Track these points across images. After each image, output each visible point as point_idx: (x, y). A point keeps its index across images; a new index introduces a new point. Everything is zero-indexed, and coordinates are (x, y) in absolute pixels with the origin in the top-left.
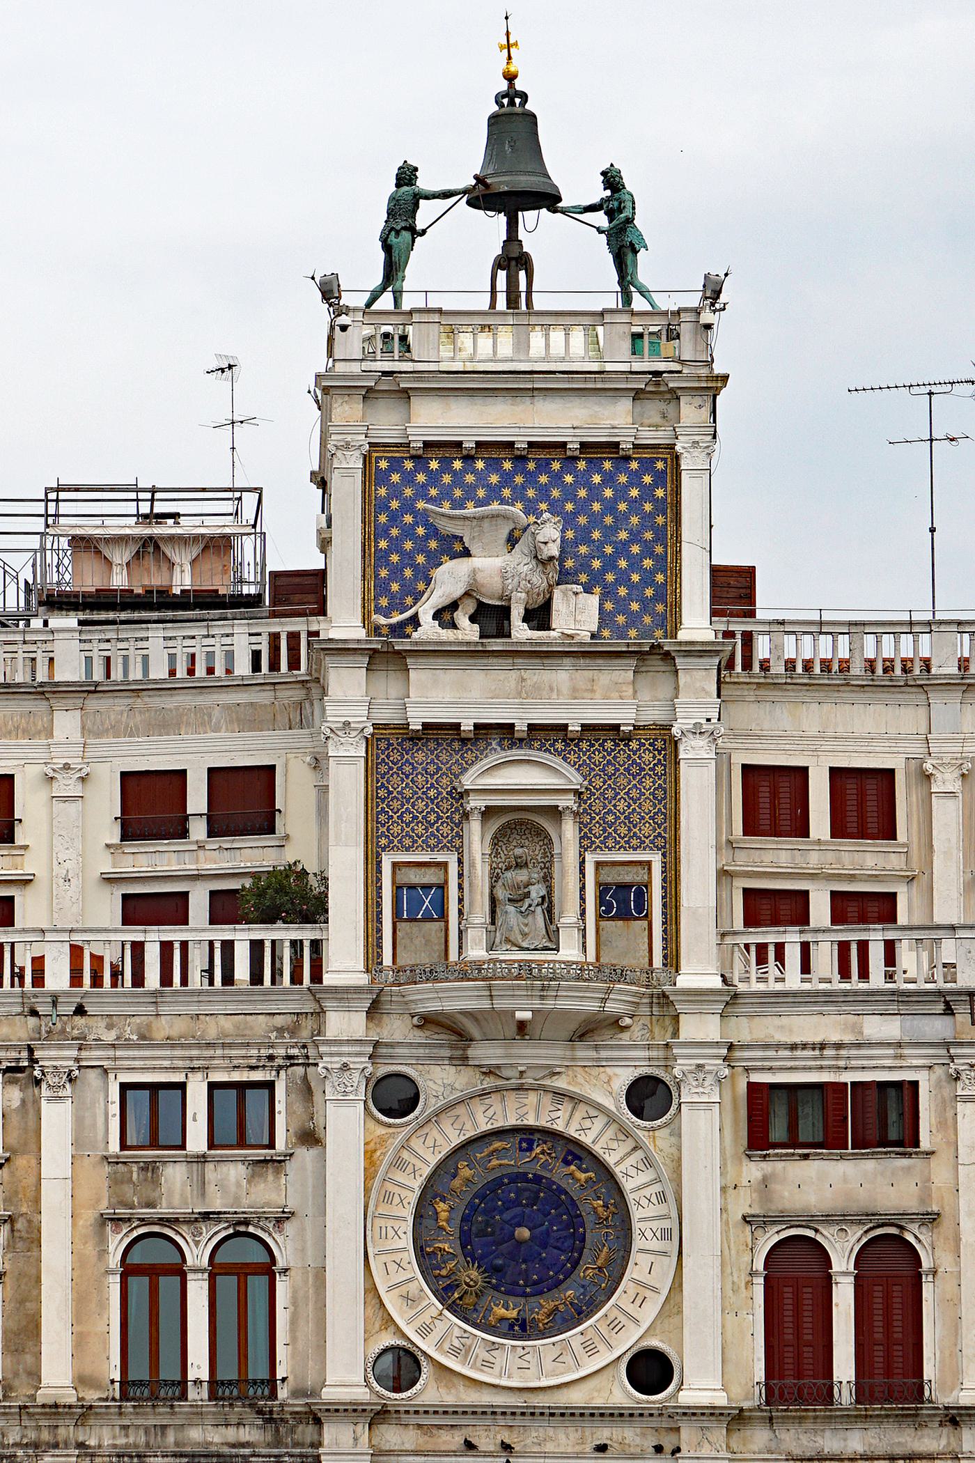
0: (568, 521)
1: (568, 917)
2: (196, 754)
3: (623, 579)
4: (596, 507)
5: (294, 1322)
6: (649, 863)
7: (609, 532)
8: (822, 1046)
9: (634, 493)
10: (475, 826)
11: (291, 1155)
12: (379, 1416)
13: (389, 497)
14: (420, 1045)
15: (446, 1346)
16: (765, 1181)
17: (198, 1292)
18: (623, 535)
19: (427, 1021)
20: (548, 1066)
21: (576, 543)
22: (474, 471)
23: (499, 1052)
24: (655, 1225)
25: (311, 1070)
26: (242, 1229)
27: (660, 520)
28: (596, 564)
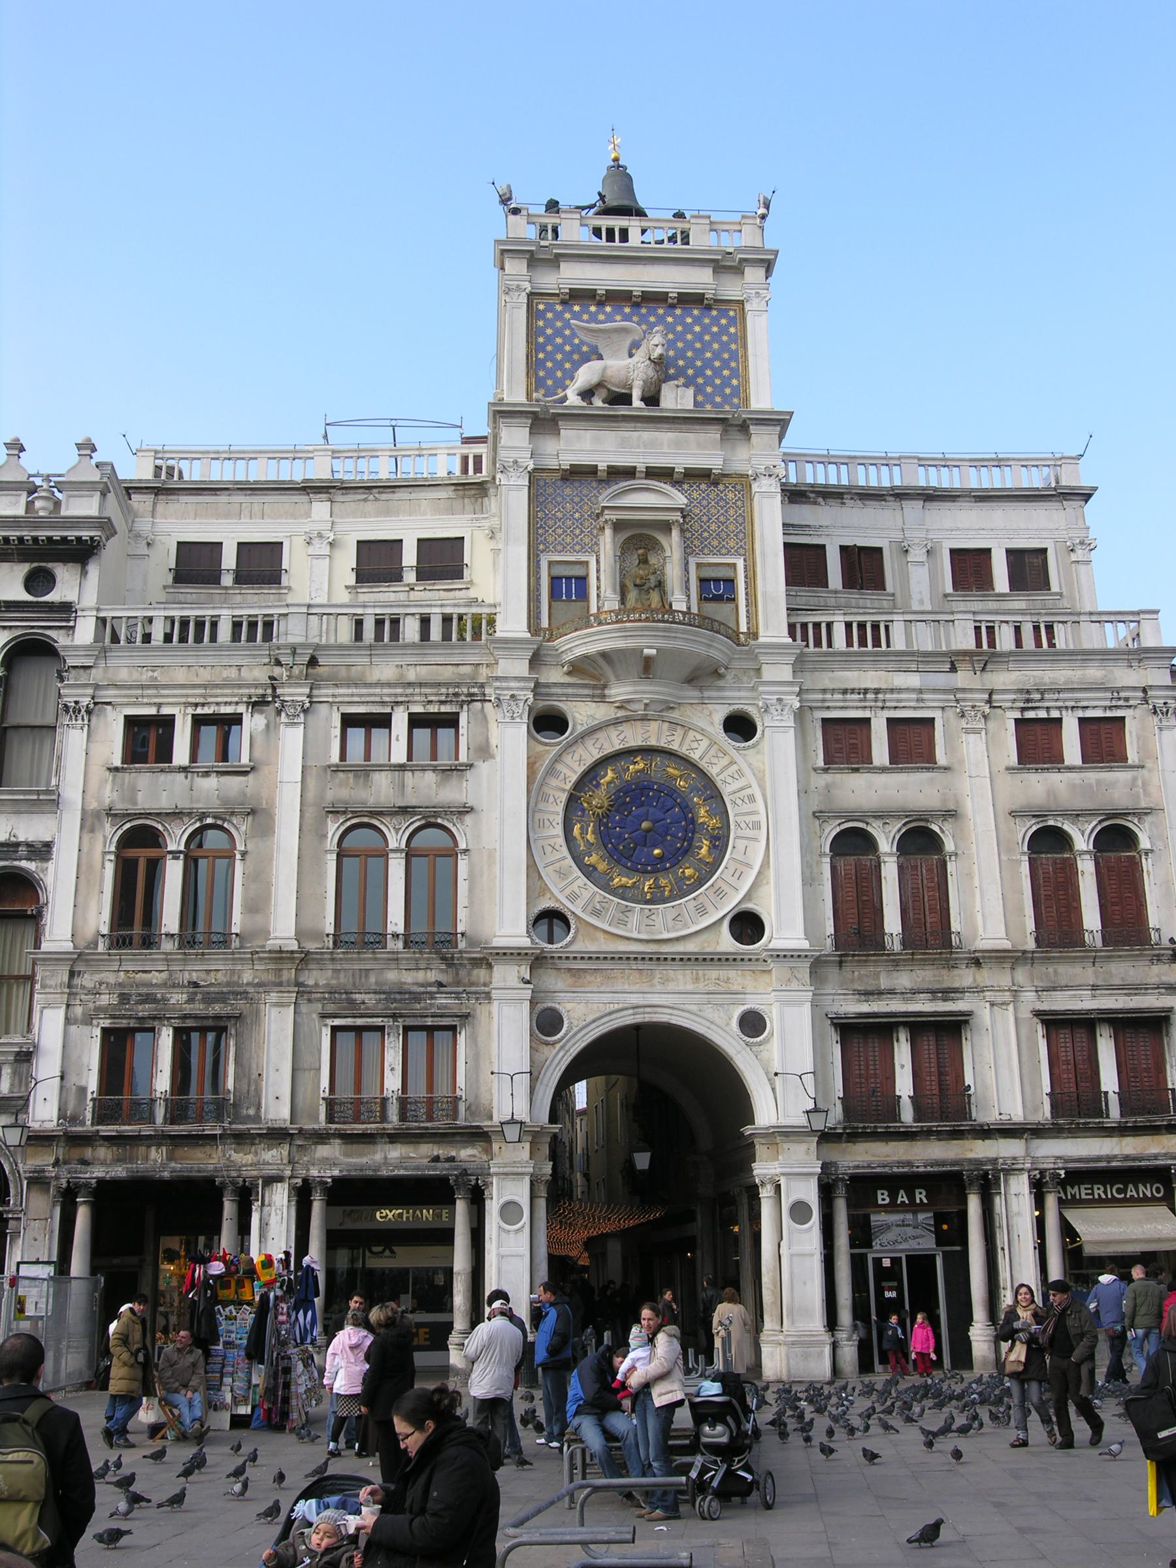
0: (670, 344)
2: (409, 527)
3: (709, 381)
4: (689, 337)
5: (471, 890)
6: (735, 564)
7: (699, 353)
8: (866, 691)
9: (715, 329)
10: (608, 532)
11: (471, 766)
12: (538, 961)
13: (546, 327)
14: (569, 685)
15: (590, 908)
16: (828, 788)
17: (396, 868)
18: (708, 355)
19: (578, 667)
20: (665, 701)
21: (676, 358)
22: (604, 313)
23: (629, 689)
24: (748, 818)
25: (488, 705)
26: (432, 820)
27: (733, 347)
28: (690, 372)
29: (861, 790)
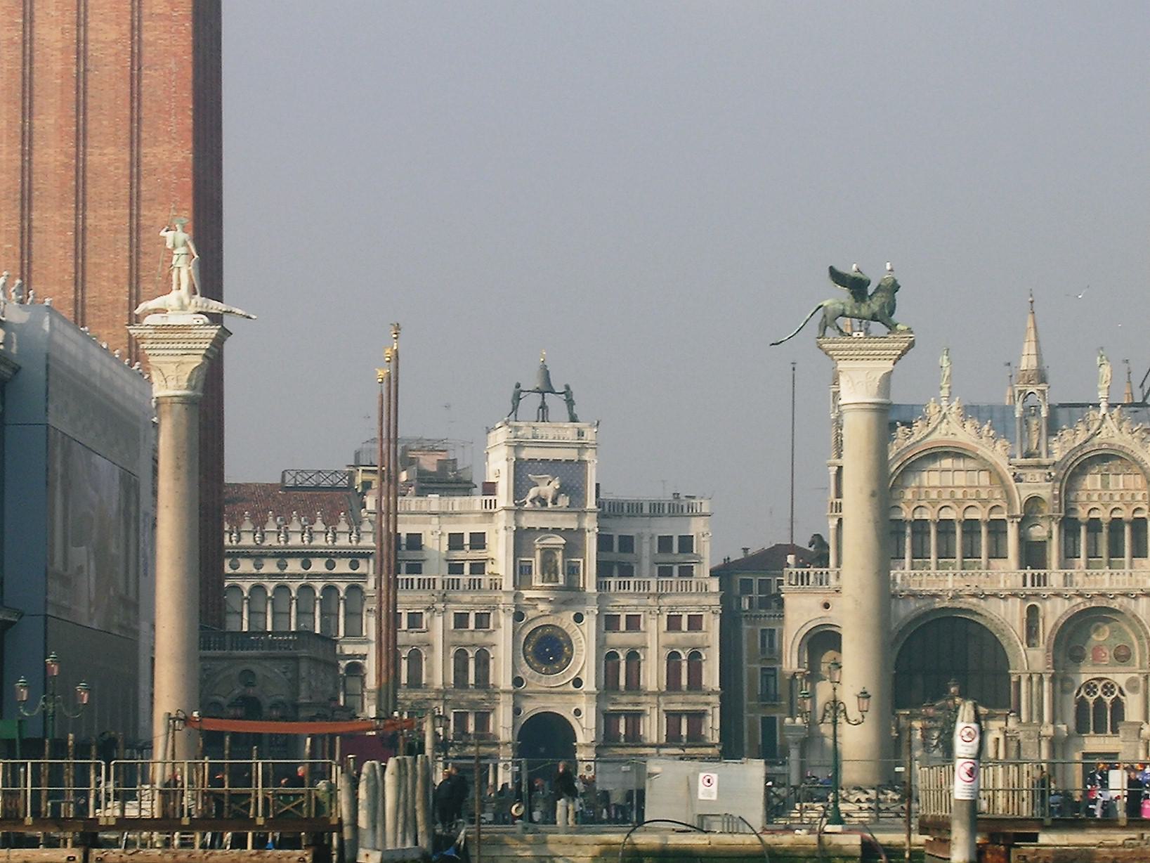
1: (561, 575)
2: (467, 529)
29: (615, 638)
